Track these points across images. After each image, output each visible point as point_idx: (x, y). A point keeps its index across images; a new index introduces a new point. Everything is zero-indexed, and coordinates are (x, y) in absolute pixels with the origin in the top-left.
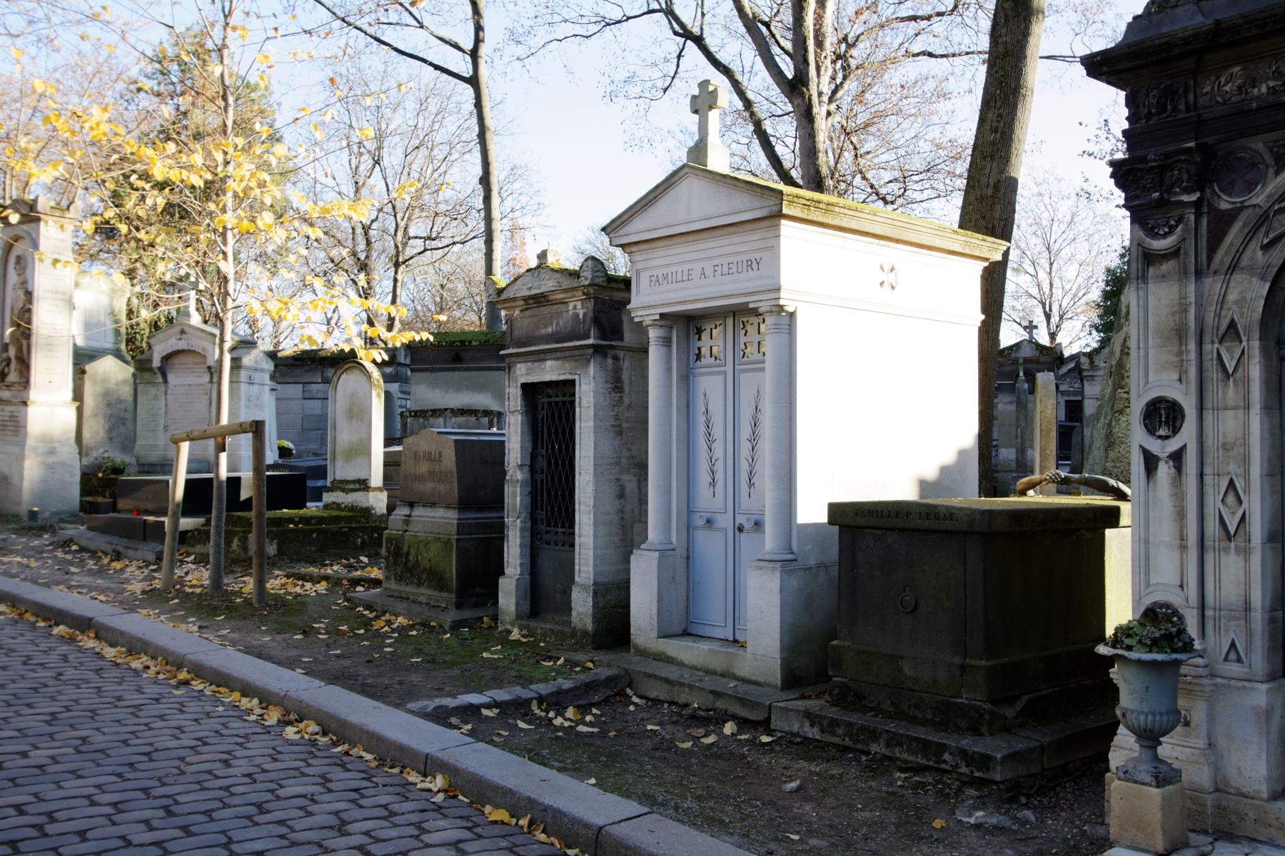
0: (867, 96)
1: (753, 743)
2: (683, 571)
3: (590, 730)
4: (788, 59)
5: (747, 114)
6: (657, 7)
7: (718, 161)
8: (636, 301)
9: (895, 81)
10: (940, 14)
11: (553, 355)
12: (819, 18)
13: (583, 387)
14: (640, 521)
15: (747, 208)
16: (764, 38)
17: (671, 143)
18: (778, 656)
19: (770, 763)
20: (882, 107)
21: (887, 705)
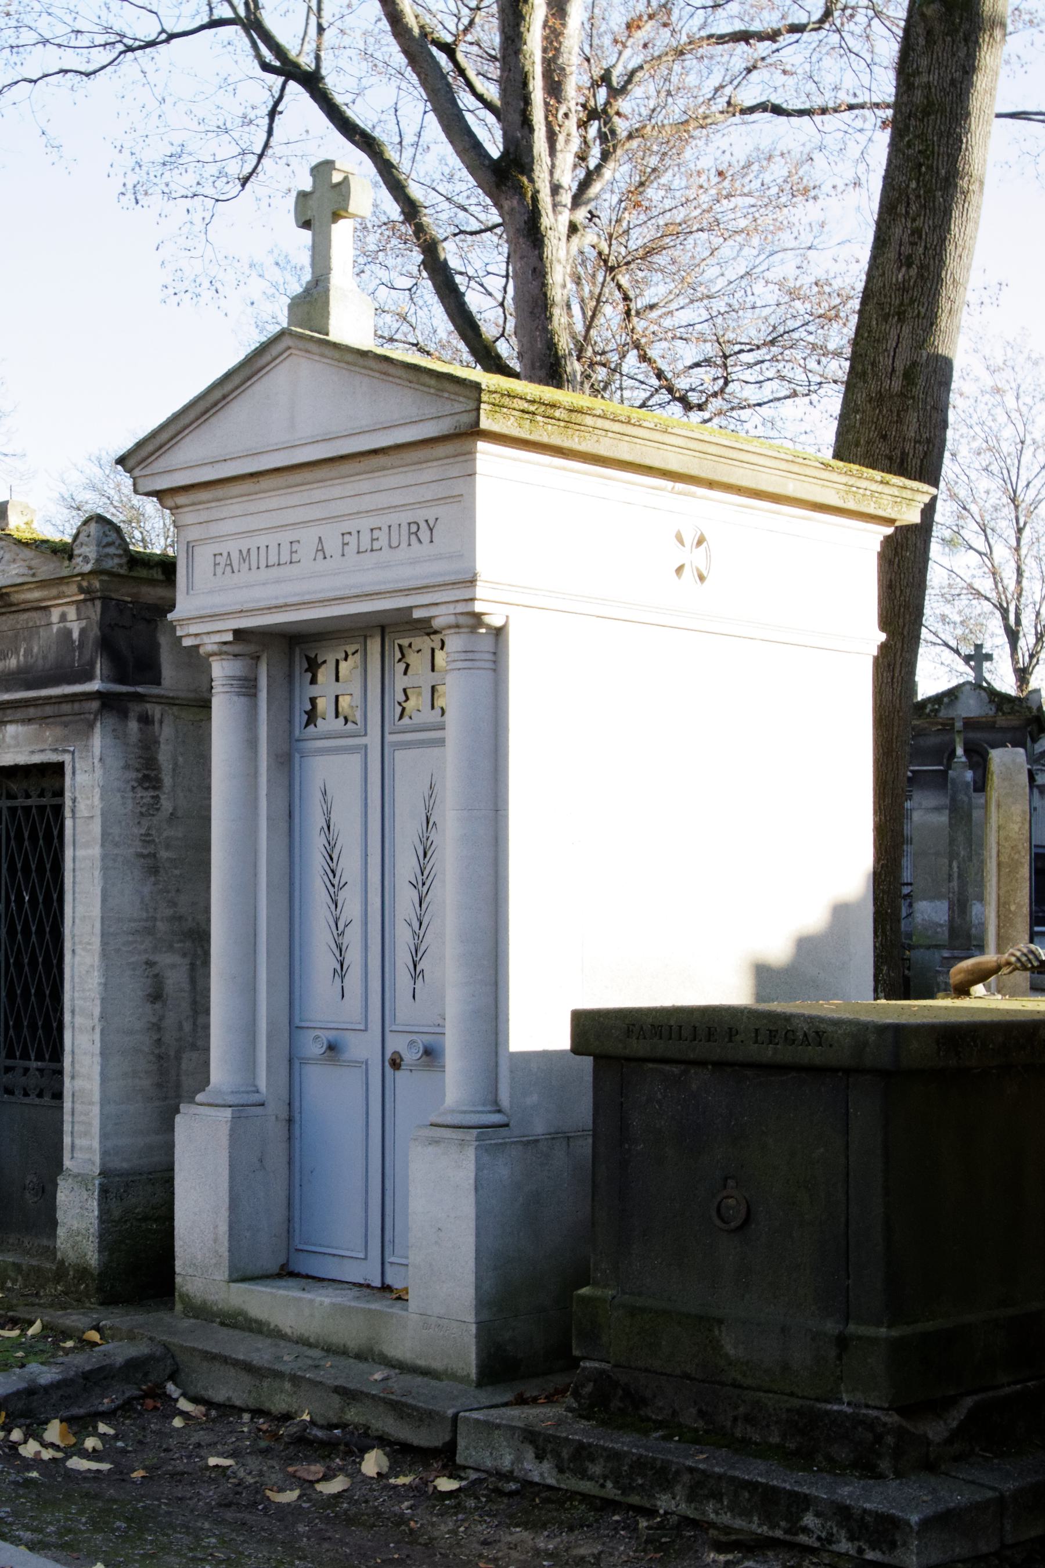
0: (650, 192)
1: (421, 1492)
2: (280, 1146)
3: (94, 1466)
4: (491, 118)
5: (408, 230)
6: (229, 14)
7: (351, 323)
8: (187, 604)
9: (706, 163)
10: (796, 29)
11: (20, 714)
12: (553, 37)
13: (80, 778)
14: (194, 1047)
15: (408, 417)
16: (444, 77)
17: (256, 287)
18: (471, 1318)
19: (454, 1532)
20: (679, 215)
21: (689, 1417)
